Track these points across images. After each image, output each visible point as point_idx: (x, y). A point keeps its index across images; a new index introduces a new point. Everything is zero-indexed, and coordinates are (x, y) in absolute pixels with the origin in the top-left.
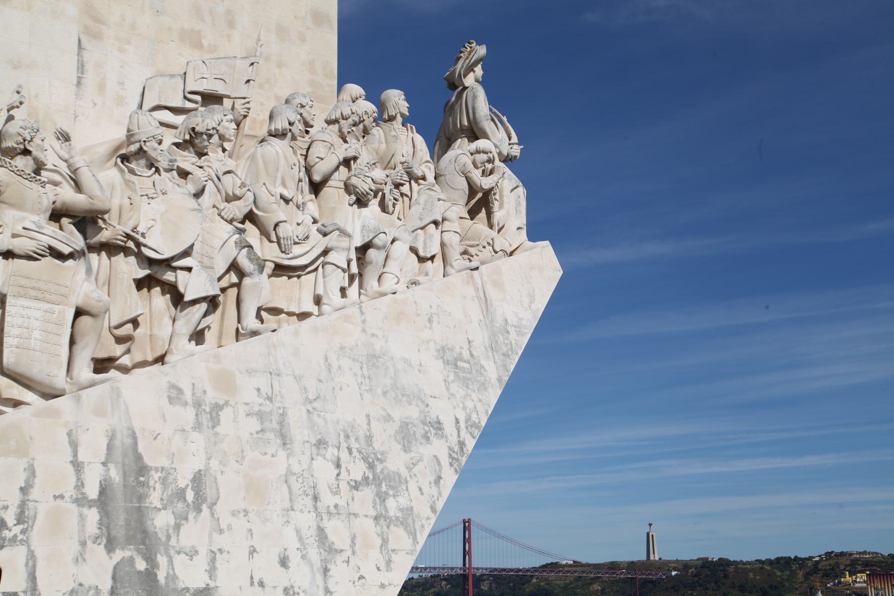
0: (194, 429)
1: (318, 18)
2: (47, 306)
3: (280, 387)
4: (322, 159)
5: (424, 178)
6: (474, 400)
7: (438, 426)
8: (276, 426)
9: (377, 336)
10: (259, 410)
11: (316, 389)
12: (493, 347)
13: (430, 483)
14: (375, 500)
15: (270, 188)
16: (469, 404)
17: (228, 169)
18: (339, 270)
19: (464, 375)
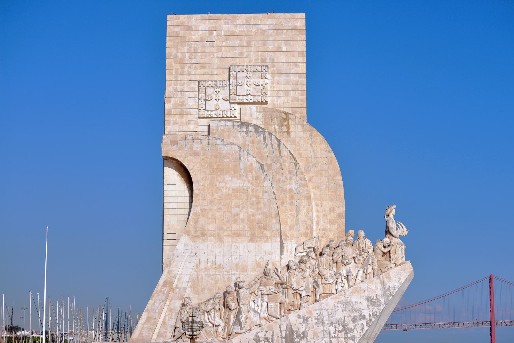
0: (303, 323)
1: (339, 216)
5: (368, 252)
7: (364, 317)
8: (321, 321)
15: (322, 267)
16: (374, 310)
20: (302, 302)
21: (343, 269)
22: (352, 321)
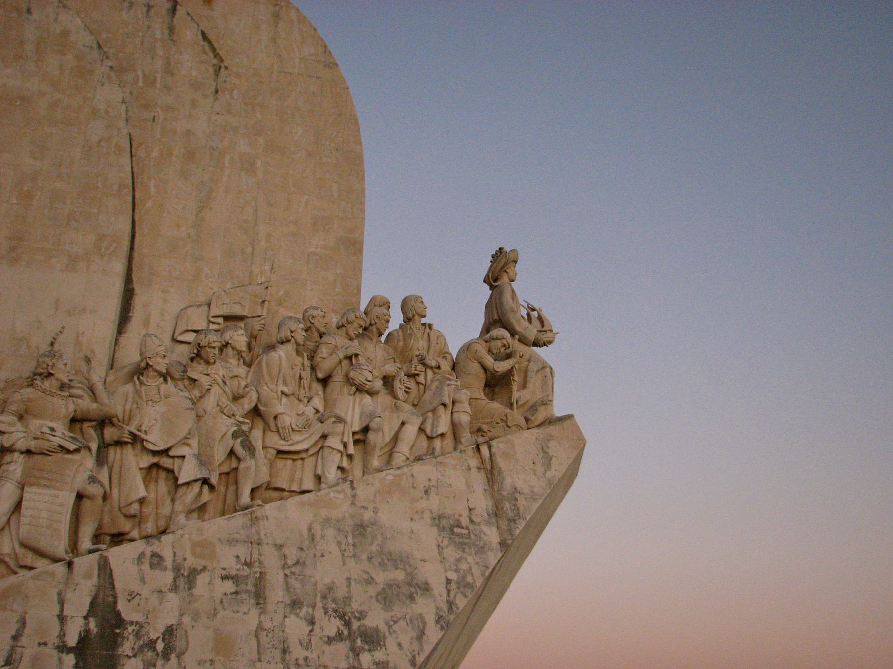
2: (53, 492)
3: (260, 555)
4: (324, 358)
5: (439, 367)
6: (470, 562)
8: (250, 587)
9: (366, 508)
10: (235, 575)
11: (296, 556)
12: (496, 513)
13: (412, 639)
14: (349, 654)
16: (464, 566)
17: (234, 374)
18: (335, 452)
19: (461, 540)
20: (178, 507)
21: (351, 404)
22: (377, 600)
